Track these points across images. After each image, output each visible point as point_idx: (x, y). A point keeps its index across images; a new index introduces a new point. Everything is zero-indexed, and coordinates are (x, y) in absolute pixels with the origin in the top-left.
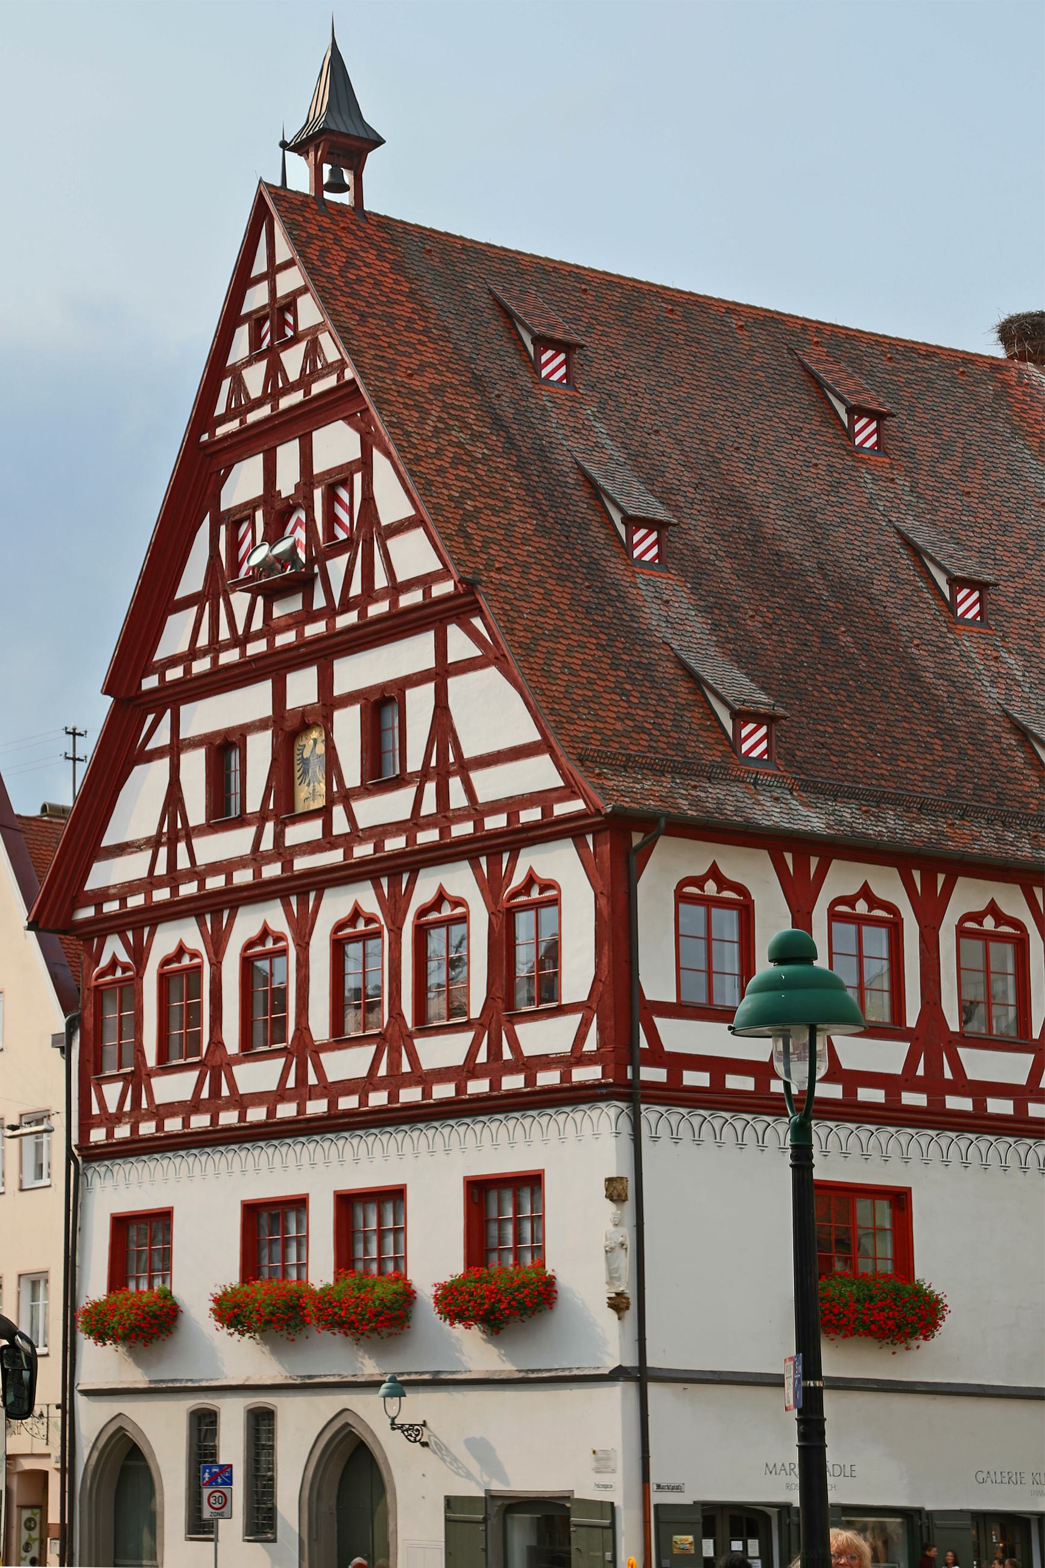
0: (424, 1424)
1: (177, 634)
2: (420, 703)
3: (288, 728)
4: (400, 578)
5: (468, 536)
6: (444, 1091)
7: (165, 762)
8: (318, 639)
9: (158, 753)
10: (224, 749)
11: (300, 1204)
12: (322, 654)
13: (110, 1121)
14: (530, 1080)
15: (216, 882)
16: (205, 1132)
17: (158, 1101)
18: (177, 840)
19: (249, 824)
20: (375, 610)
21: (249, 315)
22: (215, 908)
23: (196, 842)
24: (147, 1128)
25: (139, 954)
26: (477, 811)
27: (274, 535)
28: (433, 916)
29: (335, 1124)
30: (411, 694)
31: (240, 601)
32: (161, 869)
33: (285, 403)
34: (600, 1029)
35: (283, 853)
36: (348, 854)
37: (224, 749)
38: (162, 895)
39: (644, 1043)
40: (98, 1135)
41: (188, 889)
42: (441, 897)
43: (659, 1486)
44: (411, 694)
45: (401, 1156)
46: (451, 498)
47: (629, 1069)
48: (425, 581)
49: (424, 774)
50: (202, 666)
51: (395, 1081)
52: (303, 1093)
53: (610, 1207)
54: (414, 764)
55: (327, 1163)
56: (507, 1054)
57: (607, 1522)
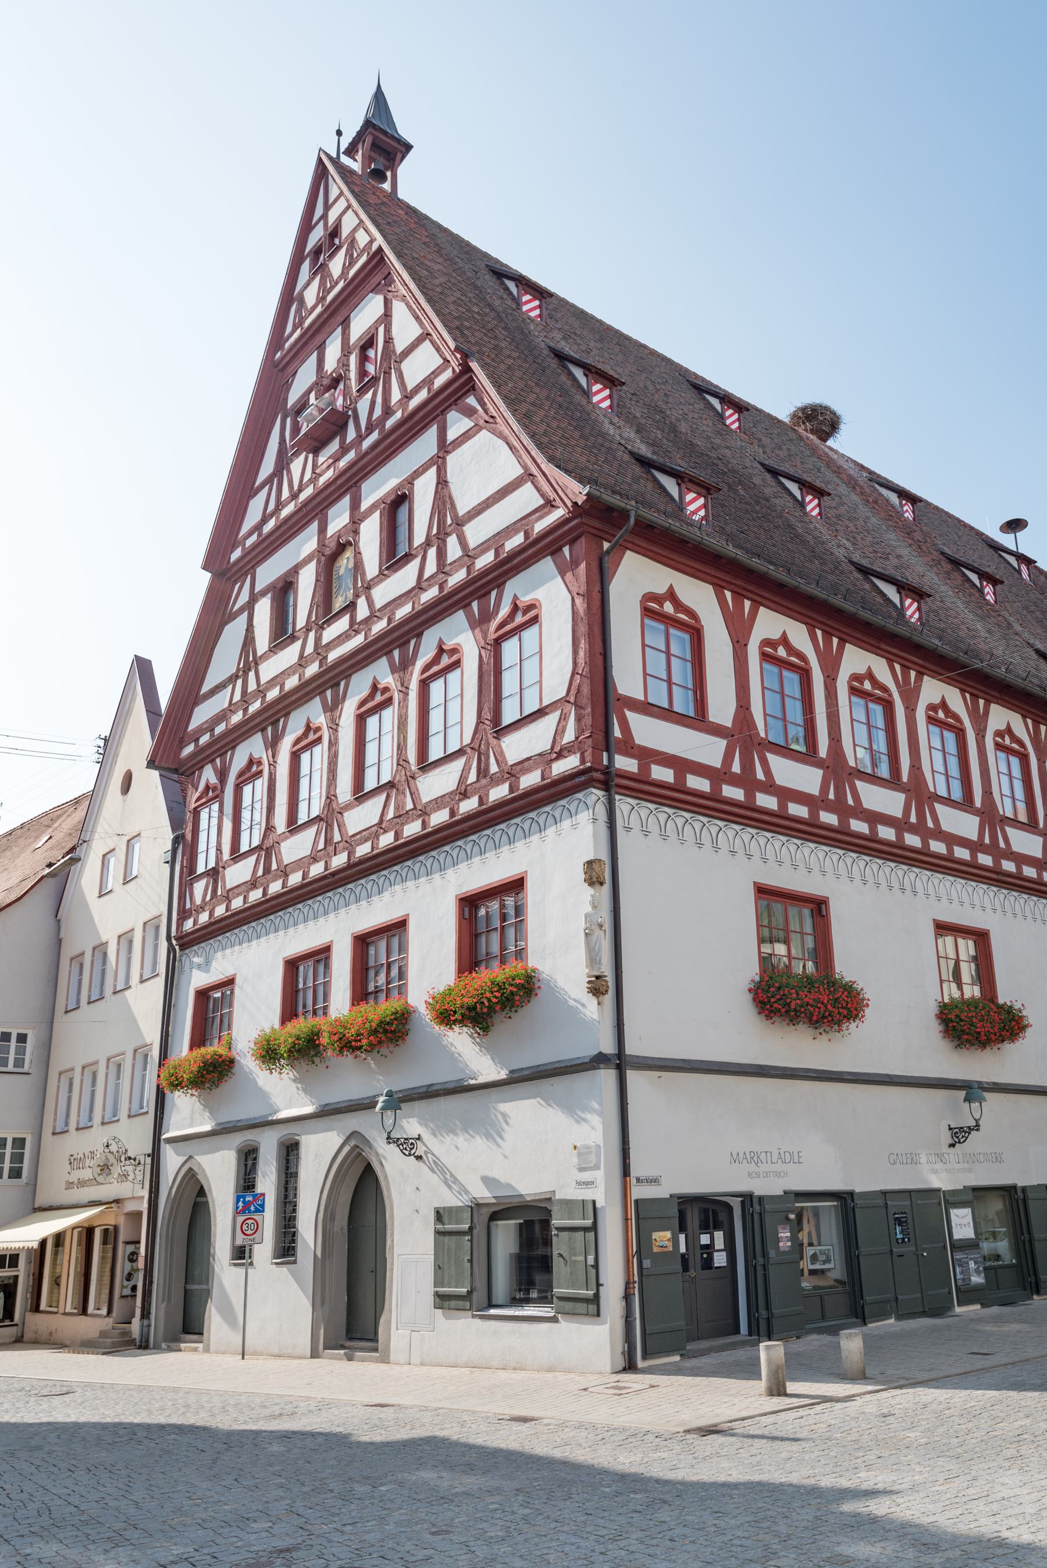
0: (419, 1138)
9: (241, 610)
18: (249, 670)
23: (262, 667)
25: (222, 775)
28: (435, 669)
34: (579, 719)
39: (617, 733)
43: (638, 1180)
47: (605, 754)
49: (428, 544)
53: (589, 891)
54: (419, 539)
57: (589, 1222)
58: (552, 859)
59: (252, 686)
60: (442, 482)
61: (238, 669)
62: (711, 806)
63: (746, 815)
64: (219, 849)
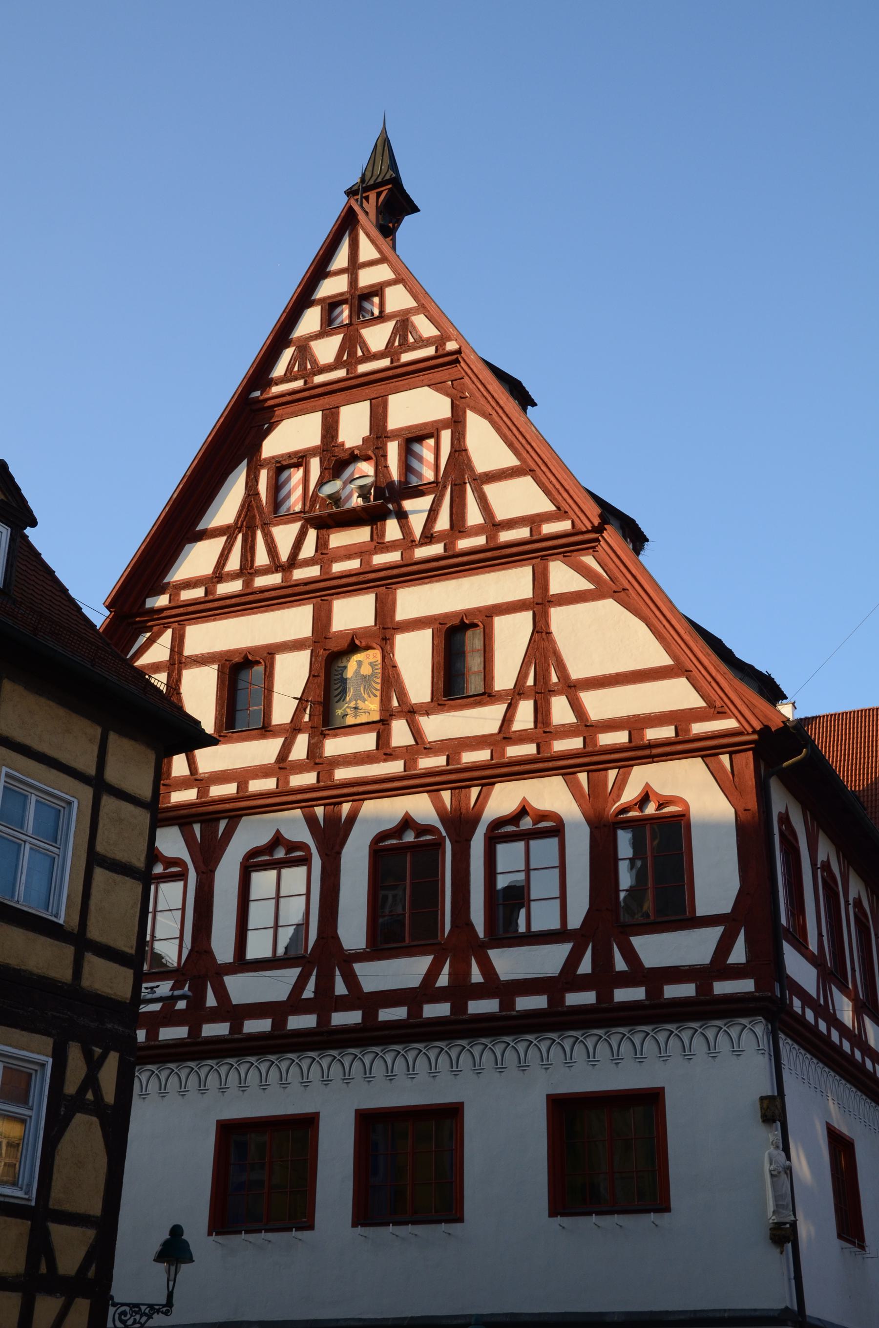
1: (197, 560)
4: (501, 515)
11: (308, 1124)
12: (383, 583)
16: (177, 1044)
20: (464, 544)
26: (586, 727)
28: (511, 828)
29: (371, 1036)
30: (499, 622)
44: (499, 622)
45: (456, 1073)
48: (534, 521)
49: (518, 693)
58: (710, 1084)
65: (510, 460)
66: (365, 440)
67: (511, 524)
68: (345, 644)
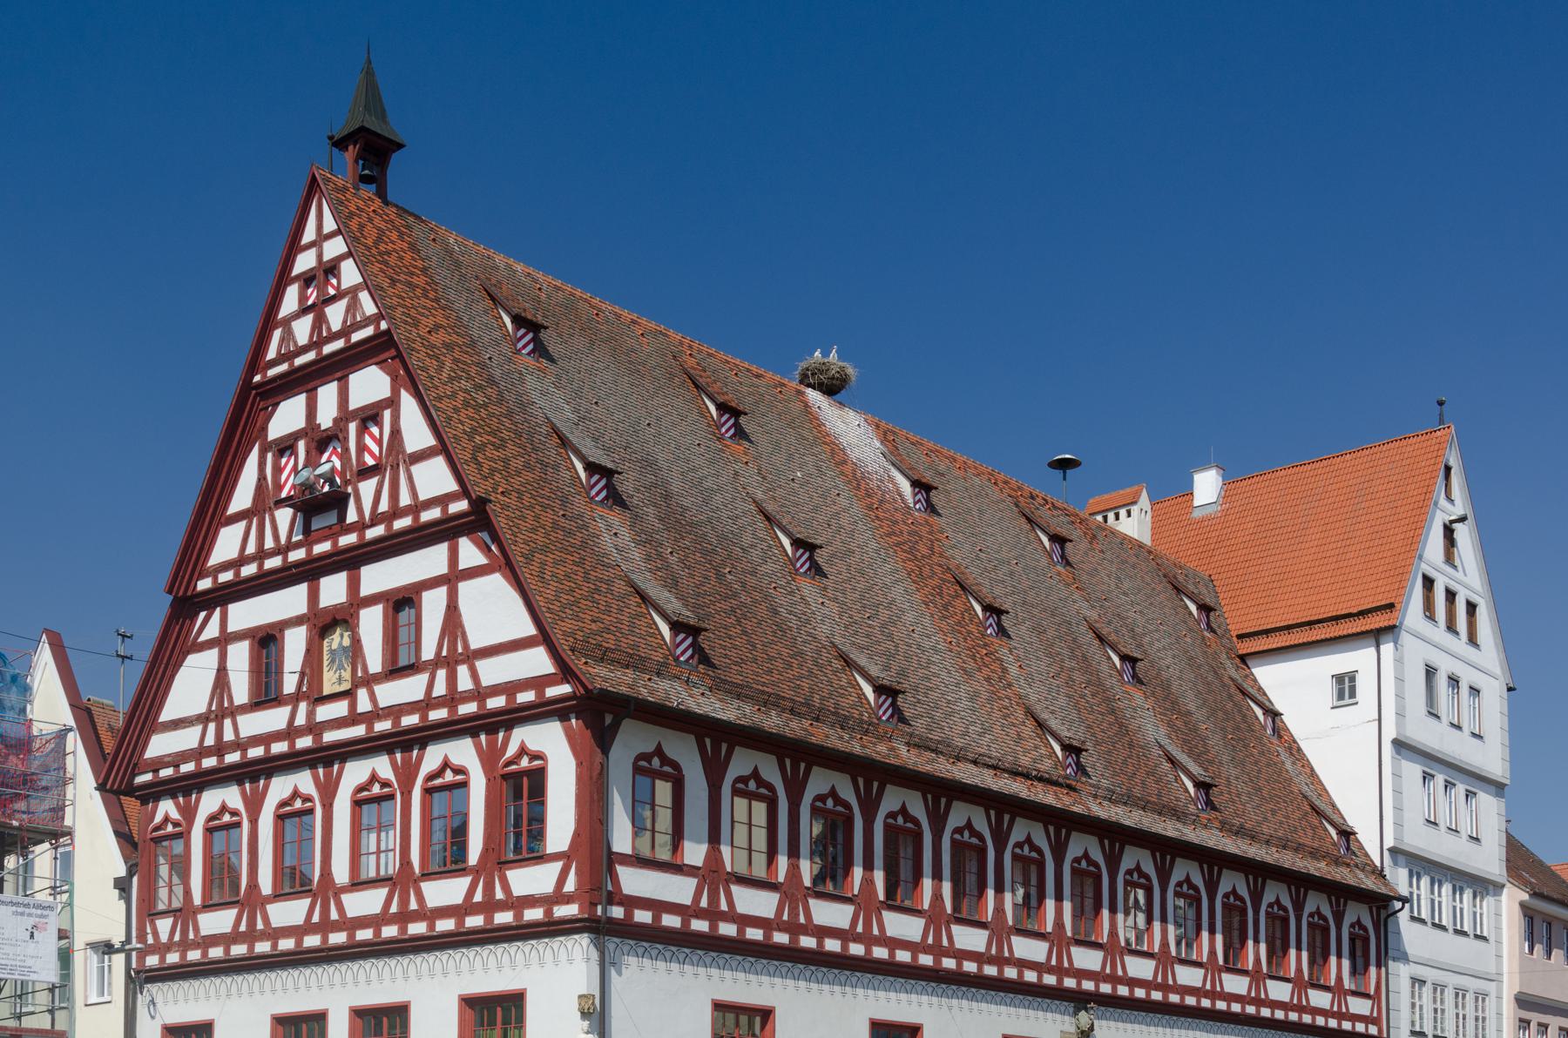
1: (227, 544)
2: (433, 604)
3: (324, 623)
4: (422, 497)
5: (479, 464)
6: (445, 925)
7: (212, 655)
8: (350, 549)
9: (210, 644)
10: (266, 640)
12: (351, 561)
13: (162, 949)
14: (518, 916)
15: (256, 752)
17: (203, 933)
18: (223, 717)
19: (285, 704)
21: (298, 277)
22: (253, 773)
23: (240, 719)
24: (194, 955)
25: (189, 813)
26: (480, 694)
27: (312, 462)
31: (284, 516)
32: (210, 740)
33: (328, 349)
35: (314, 728)
36: (370, 728)
37: (266, 640)
38: (209, 762)
40: (152, 961)
41: (233, 758)
42: (446, 765)
46: (465, 432)
48: (443, 500)
49: (437, 662)
50: (249, 570)
51: (404, 917)
52: (326, 927)
54: (428, 653)
55: (344, 984)
56: (499, 895)
59: (229, 735)
60: (452, 610)
61: (209, 711)
62: (683, 941)
63: (712, 945)
64: (188, 893)
65: (430, 441)
66: (335, 420)
67: (429, 504)
68: (329, 619)
